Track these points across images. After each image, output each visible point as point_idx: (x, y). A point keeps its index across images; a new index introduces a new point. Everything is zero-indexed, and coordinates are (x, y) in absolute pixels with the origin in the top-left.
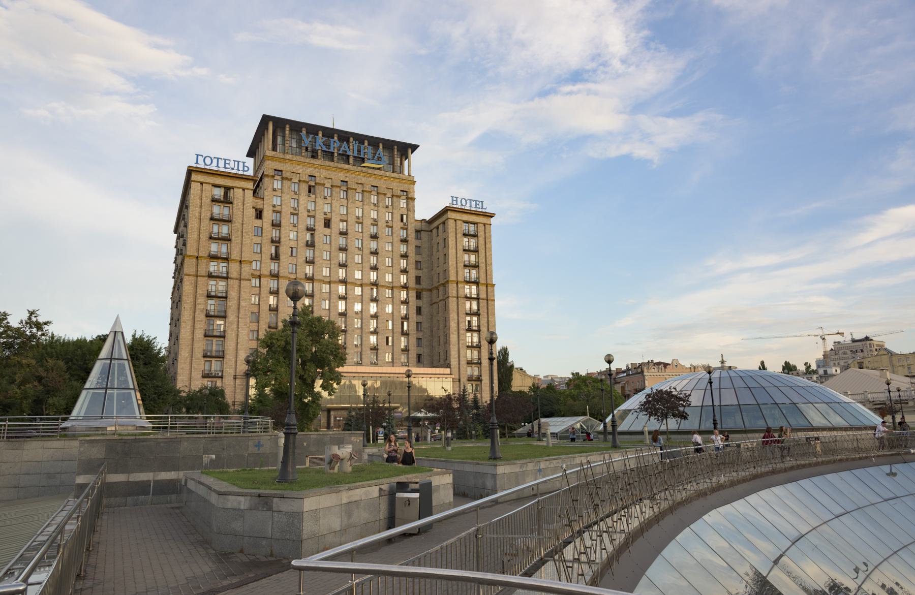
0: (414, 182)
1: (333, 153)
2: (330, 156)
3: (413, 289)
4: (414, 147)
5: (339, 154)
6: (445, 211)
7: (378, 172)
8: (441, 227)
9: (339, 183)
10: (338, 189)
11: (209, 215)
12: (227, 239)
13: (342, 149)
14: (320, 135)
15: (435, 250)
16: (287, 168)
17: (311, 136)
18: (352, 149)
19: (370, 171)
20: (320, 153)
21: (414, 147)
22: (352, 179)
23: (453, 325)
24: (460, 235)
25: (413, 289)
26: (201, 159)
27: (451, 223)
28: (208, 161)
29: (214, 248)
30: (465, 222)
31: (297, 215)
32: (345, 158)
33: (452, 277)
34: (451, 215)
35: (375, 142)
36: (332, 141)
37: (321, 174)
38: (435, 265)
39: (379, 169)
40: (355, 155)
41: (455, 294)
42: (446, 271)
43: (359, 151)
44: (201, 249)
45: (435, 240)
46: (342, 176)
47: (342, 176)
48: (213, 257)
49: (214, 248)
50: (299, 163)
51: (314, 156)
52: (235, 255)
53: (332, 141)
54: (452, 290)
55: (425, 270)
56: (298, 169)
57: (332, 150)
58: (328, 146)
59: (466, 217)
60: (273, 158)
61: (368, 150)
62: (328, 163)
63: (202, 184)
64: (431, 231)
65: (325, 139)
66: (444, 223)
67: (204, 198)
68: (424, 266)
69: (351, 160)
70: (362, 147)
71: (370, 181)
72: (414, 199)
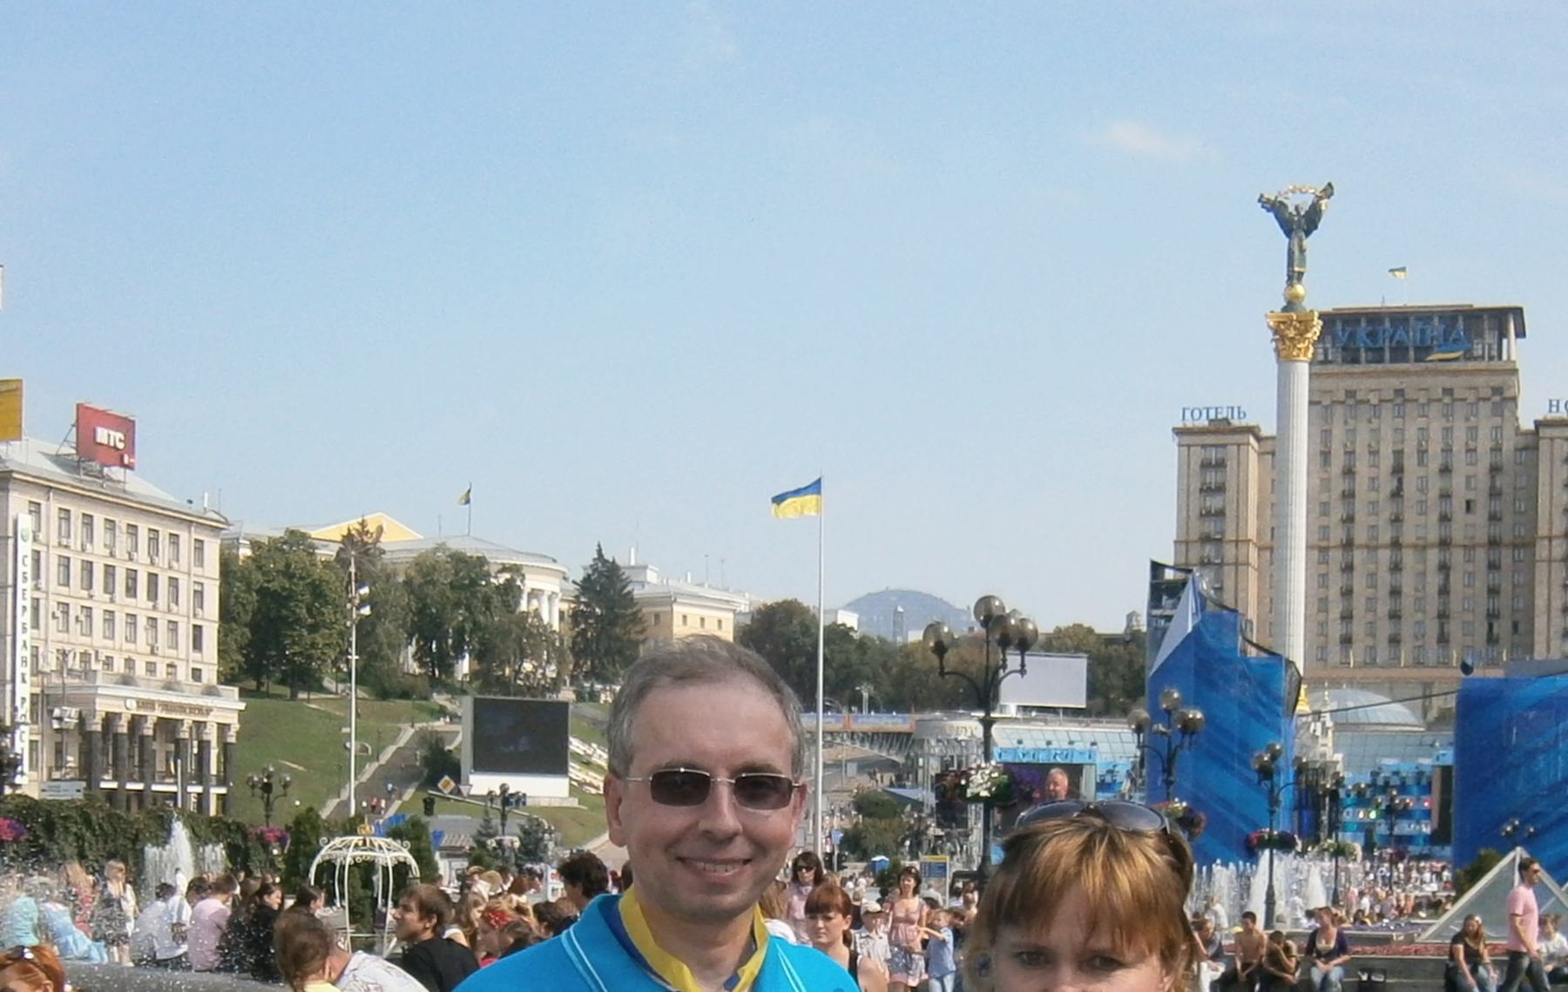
0: (1515, 371)
1: (1382, 349)
5: (1392, 350)
7: (1454, 366)
10: (1390, 405)
11: (1199, 485)
12: (1221, 513)
13: (1397, 338)
14: (1363, 324)
17: (1349, 329)
18: (1411, 337)
19: (1440, 365)
20: (1363, 355)
23: (1540, 603)
24: (1558, 463)
26: (1188, 413)
27: (1544, 446)
28: (1196, 414)
29: (1210, 527)
32: (1399, 353)
33: (1543, 530)
34: (1543, 432)
37: (1362, 386)
39: (1456, 359)
41: (1545, 554)
46: (1395, 383)
47: (1395, 383)
48: (1206, 539)
49: (1210, 527)
51: (1355, 361)
54: (1542, 551)
57: (1380, 344)
62: (1373, 366)
63: (1189, 446)
69: (1412, 353)
71: (1437, 384)
72: (1514, 399)
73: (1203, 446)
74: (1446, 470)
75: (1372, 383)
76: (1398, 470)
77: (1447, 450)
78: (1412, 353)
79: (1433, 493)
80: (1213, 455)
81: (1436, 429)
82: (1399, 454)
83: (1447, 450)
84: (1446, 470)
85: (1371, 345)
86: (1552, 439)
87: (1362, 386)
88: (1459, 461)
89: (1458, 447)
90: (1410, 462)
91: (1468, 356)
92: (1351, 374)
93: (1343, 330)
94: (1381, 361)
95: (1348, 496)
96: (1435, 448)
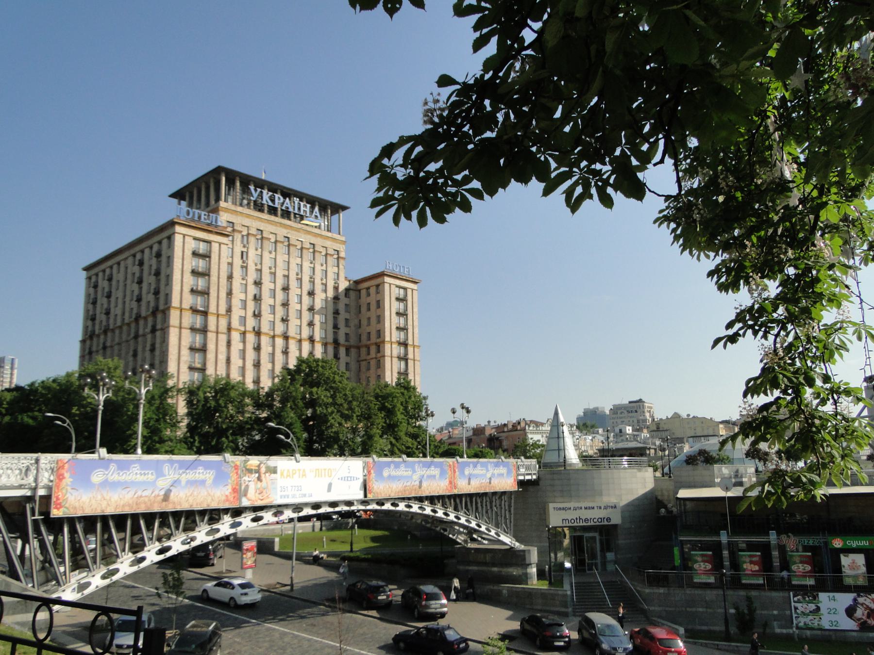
2: (273, 211)
3: (343, 345)
4: (344, 208)
5: (282, 210)
6: (382, 275)
7: (317, 231)
8: (373, 290)
9: (282, 239)
13: (285, 205)
15: (364, 309)
16: (238, 220)
17: (259, 190)
21: (344, 208)
22: (294, 236)
24: (393, 299)
25: (343, 345)
30: (397, 286)
31: (246, 267)
32: (286, 214)
34: (387, 279)
35: (312, 201)
36: (277, 196)
37: (267, 228)
38: (364, 322)
40: (296, 211)
42: (380, 333)
43: (299, 209)
44: (184, 301)
45: (364, 299)
50: (248, 216)
52: (212, 309)
53: (277, 196)
55: (353, 328)
56: (247, 222)
57: (276, 205)
58: (273, 201)
59: (398, 282)
60: (227, 210)
61: (305, 208)
62: (273, 218)
63: (184, 236)
64: (359, 291)
65: (271, 193)
66: (378, 286)
67: (186, 251)
68: (352, 324)
69: (292, 215)
70: (302, 204)
71: (307, 240)
73: (195, 239)
74: (311, 294)
75: (273, 229)
76: (286, 289)
77: (312, 282)
78: (292, 215)
79: (305, 307)
80: (202, 248)
81: (306, 265)
82: (287, 277)
83: (312, 282)
84: (311, 294)
85: (271, 204)
86: (390, 284)
87: (267, 228)
88: (318, 288)
89: (318, 282)
90: (293, 284)
91: (319, 227)
92: (260, 219)
93: (256, 190)
94: (276, 215)
95: (257, 299)
96: (306, 279)
